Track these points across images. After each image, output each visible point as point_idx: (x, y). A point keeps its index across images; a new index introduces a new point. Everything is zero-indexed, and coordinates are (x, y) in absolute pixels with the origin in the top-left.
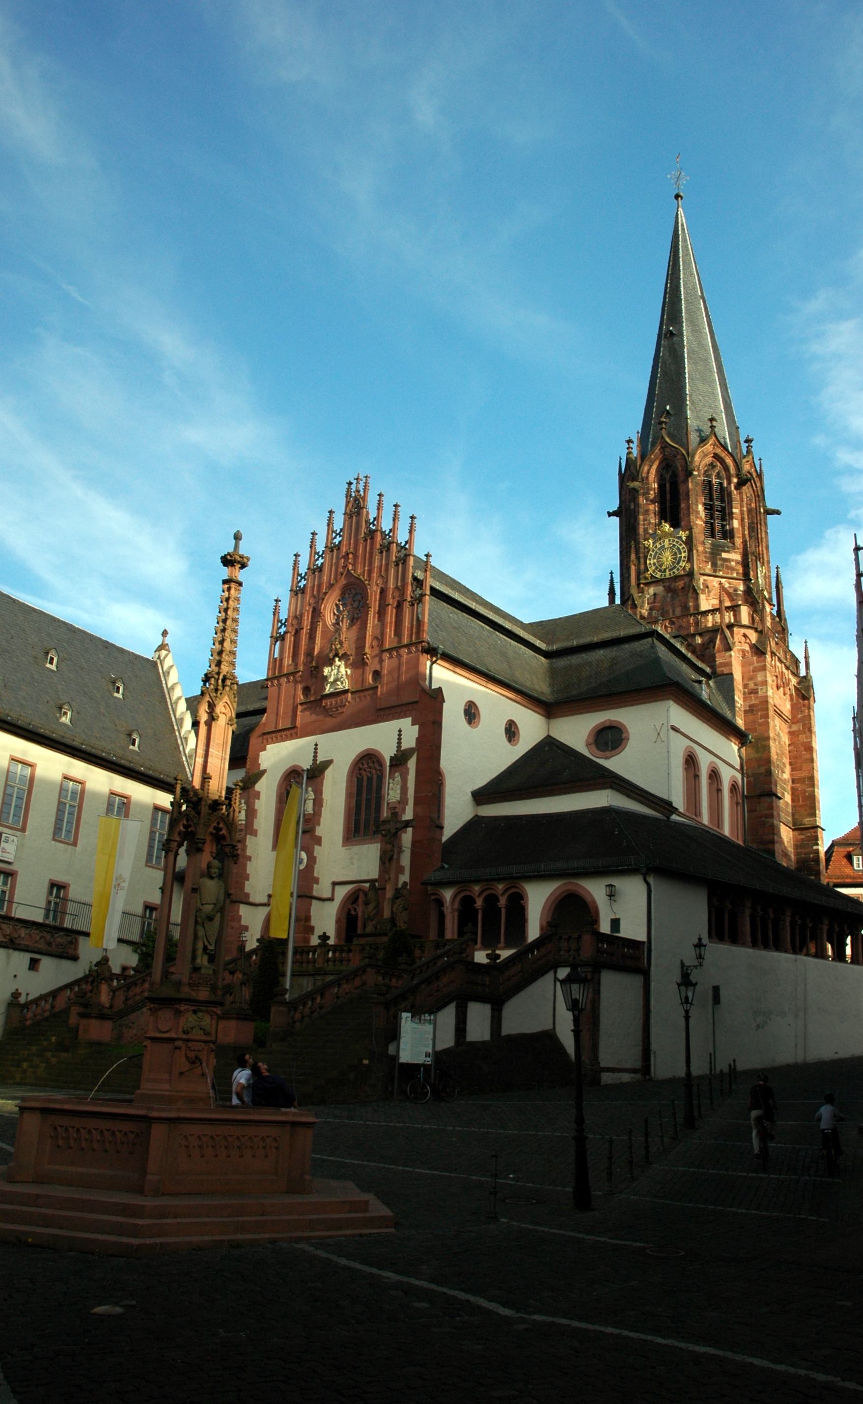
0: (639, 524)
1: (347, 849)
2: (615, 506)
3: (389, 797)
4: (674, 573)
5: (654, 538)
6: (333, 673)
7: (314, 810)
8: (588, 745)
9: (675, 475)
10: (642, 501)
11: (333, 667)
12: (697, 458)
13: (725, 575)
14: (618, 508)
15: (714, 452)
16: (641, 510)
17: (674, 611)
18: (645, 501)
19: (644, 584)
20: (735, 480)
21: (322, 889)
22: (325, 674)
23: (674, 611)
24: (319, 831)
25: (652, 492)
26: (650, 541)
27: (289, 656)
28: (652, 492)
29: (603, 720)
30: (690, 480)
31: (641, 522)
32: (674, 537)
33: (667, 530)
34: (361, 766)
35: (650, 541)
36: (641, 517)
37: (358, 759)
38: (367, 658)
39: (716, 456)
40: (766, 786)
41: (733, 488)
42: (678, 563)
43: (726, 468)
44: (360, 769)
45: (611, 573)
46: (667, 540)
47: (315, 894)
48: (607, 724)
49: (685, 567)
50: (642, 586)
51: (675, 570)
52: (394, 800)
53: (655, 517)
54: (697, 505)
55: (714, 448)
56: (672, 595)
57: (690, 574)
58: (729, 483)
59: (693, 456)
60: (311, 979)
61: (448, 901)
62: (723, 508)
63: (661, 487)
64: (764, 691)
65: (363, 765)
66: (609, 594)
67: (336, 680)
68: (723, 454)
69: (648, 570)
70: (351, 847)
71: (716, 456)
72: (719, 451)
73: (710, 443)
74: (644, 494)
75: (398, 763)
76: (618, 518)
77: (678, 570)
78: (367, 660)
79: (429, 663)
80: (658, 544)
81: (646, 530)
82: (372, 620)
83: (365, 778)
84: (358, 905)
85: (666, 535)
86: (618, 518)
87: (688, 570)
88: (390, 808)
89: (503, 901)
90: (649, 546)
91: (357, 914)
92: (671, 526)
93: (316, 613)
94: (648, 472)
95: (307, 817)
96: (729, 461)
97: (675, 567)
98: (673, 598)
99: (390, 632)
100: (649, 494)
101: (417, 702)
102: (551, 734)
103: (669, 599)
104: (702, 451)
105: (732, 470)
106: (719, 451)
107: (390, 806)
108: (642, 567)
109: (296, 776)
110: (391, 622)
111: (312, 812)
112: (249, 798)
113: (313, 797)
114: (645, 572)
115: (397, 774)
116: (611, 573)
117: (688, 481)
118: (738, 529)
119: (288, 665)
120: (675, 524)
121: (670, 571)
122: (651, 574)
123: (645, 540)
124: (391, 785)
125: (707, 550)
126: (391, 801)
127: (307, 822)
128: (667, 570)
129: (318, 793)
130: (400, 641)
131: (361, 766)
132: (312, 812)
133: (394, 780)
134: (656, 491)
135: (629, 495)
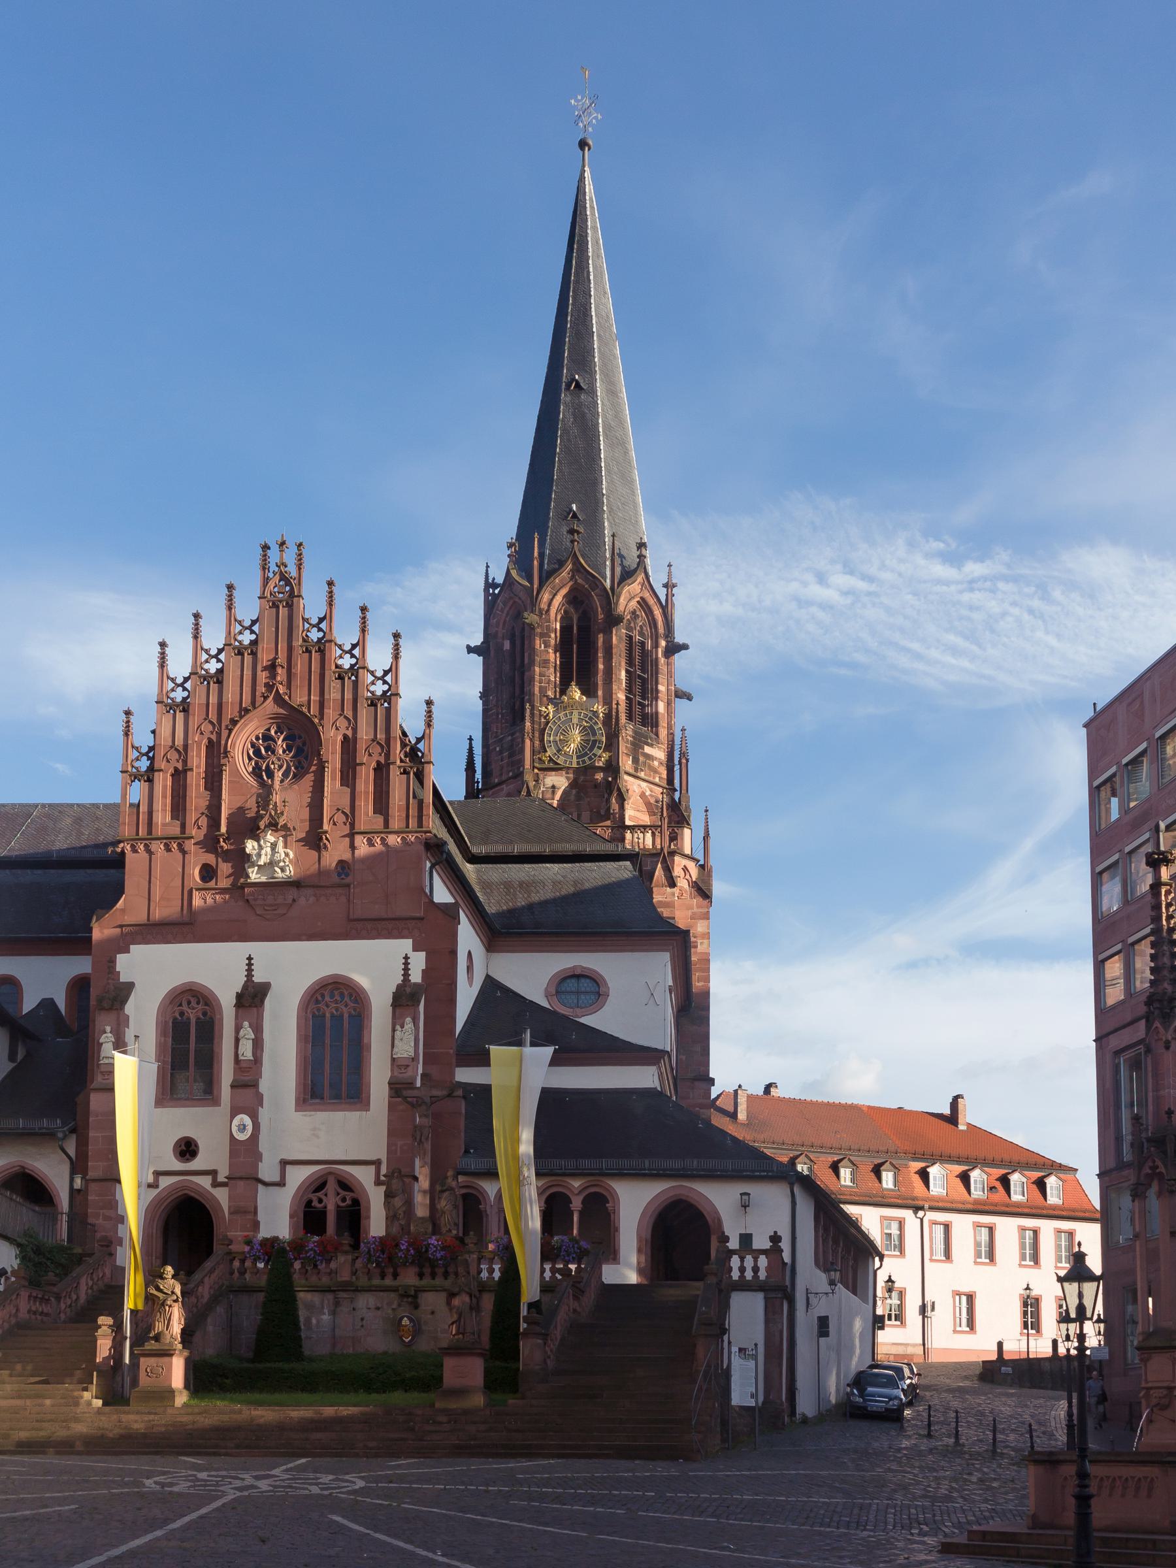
0: (532, 679)
1: (305, 1115)
2: (477, 639)
3: (395, 1050)
5: (555, 705)
6: (263, 852)
7: (254, 1054)
8: (548, 995)
9: (586, 618)
10: (539, 644)
11: (262, 842)
12: (622, 601)
13: (646, 778)
14: (482, 643)
15: (641, 595)
16: (537, 659)
17: (579, 816)
18: (543, 645)
19: (539, 769)
20: (663, 643)
21: (267, 1170)
22: (248, 851)
23: (579, 816)
24: (264, 1086)
25: (553, 635)
26: (549, 707)
27: (164, 810)
28: (553, 635)
30: (614, 632)
31: (537, 678)
32: (587, 710)
33: (577, 698)
34: (320, 998)
35: (549, 707)
36: (537, 669)
38: (327, 839)
39: (643, 603)
40: (702, 1069)
41: (660, 655)
42: (591, 749)
43: (653, 623)
44: (317, 1002)
45: (471, 739)
46: (575, 713)
47: (260, 1176)
48: (578, 972)
50: (536, 771)
51: (586, 758)
52: (405, 1056)
53: (555, 673)
54: (620, 671)
55: (642, 589)
56: (578, 793)
57: (613, 768)
58: (656, 646)
59: (619, 597)
60: (330, 1296)
61: (492, 1199)
62: (644, 681)
63: (566, 630)
64: (705, 946)
65: (323, 996)
66: (466, 770)
67: (272, 864)
68: (651, 601)
69: (545, 751)
70: (313, 1113)
71: (643, 603)
72: (647, 595)
73: (638, 581)
74: (542, 635)
76: (482, 658)
78: (325, 841)
79: (428, 865)
80: (561, 715)
81: (543, 691)
82: (332, 784)
83: (328, 1015)
85: (573, 705)
86: (482, 658)
88: (398, 1066)
89: (576, 1204)
90: (548, 715)
92: (583, 693)
93: (216, 753)
94: (550, 605)
95: (243, 1065)
96: (657, 613)
97: (587, 754)
98: (578, 798)
99: (366, 806)
100: (550, 637)
101: (422, 919)
102: (490, 974)
103: (572, 798)
104: (629, 590)
105: (661, 630)
106: (647, 595)
108: (537, 743)
109: (193, 1000)
110: (367, 793)
111: (252, 1058)
112: (119, 1024)
113: (253, 1037)
114: (539, 753)
116: (471, 739)
117: (612, 632)
118: (664, 714)
119: (164, 825)
120: (589, 690)
122: (549, 756)
123: (541, 705)
124: (398, 1033)
125: (628, 737)
126: (399, 1056)
127: (243, 1072)
129: (258, 1029)
130: (386, 824)
131: (320, 998)
132: (252, 1058)
133: (402, 1027)
134: (558, 634)
135: (503, 629)
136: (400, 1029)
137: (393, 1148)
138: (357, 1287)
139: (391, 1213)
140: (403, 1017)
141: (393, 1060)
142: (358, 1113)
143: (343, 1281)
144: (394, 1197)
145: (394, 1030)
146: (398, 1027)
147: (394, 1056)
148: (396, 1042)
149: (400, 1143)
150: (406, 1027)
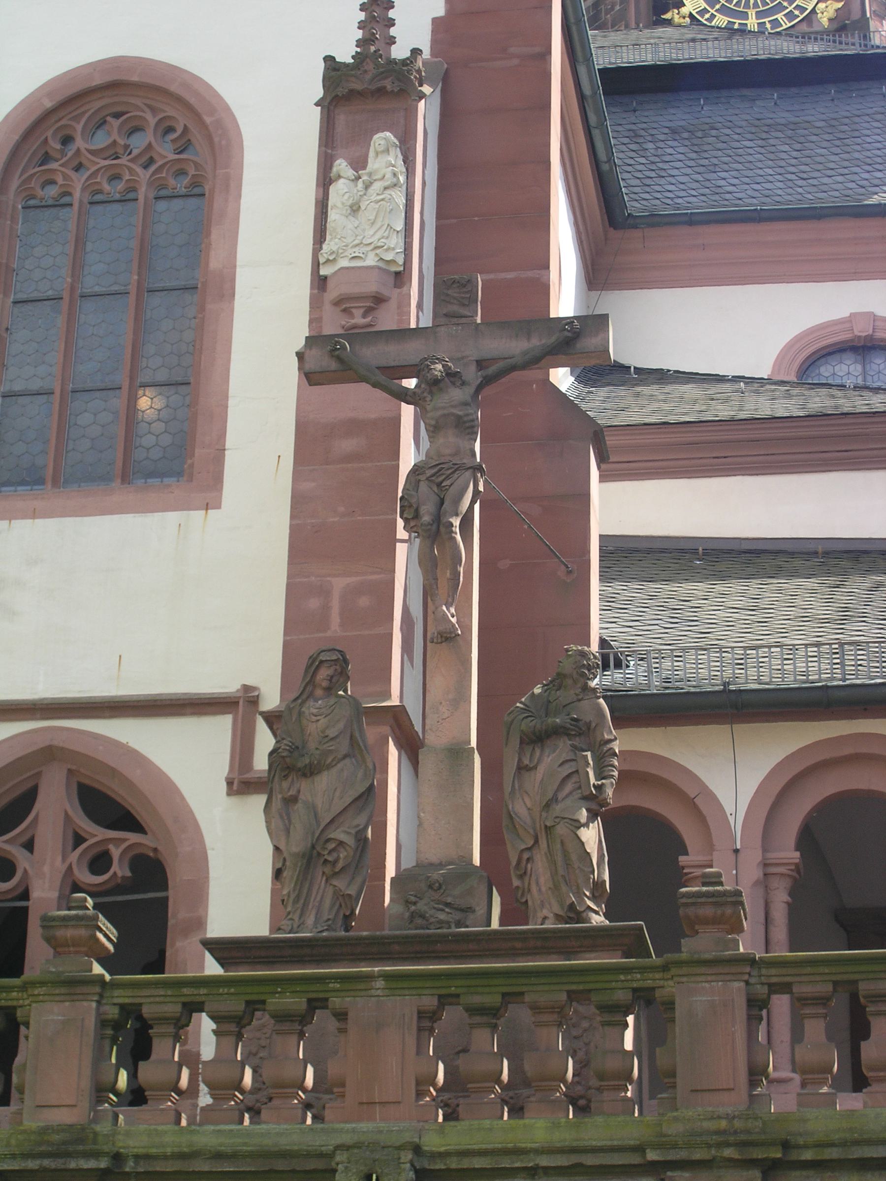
4: (775, 23)
29: (844, 313)
37: (48, 104)
48: (862, 330)
49: (813, 11)
51: (780, 16)
52: (371, 261)
75: (388, 84)
77: (790, 16)
84: (29, 846)
87: (825, 22)
91: (25, 895)
107: (333, 292)
115: (383, 138)
121: (759, 15)
122: (691, 16)
124: (340, 192)
126: (344, 263)
128: (752, 13)
133: (359, 164)
136: (351, 173)
137: (314, 603)
138: (117, 1158)
139: (297, 845)
140: (362, 137)
141: (320, 283)
142: (173, 517)
143: (45, 1130)
144: (310, 771)
145: (325, 180)
146: (341, 166)
147: (323, 272)
148: (333, 216)
149: (339, 584)
150: (375, 164)
